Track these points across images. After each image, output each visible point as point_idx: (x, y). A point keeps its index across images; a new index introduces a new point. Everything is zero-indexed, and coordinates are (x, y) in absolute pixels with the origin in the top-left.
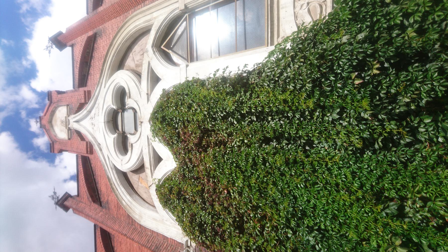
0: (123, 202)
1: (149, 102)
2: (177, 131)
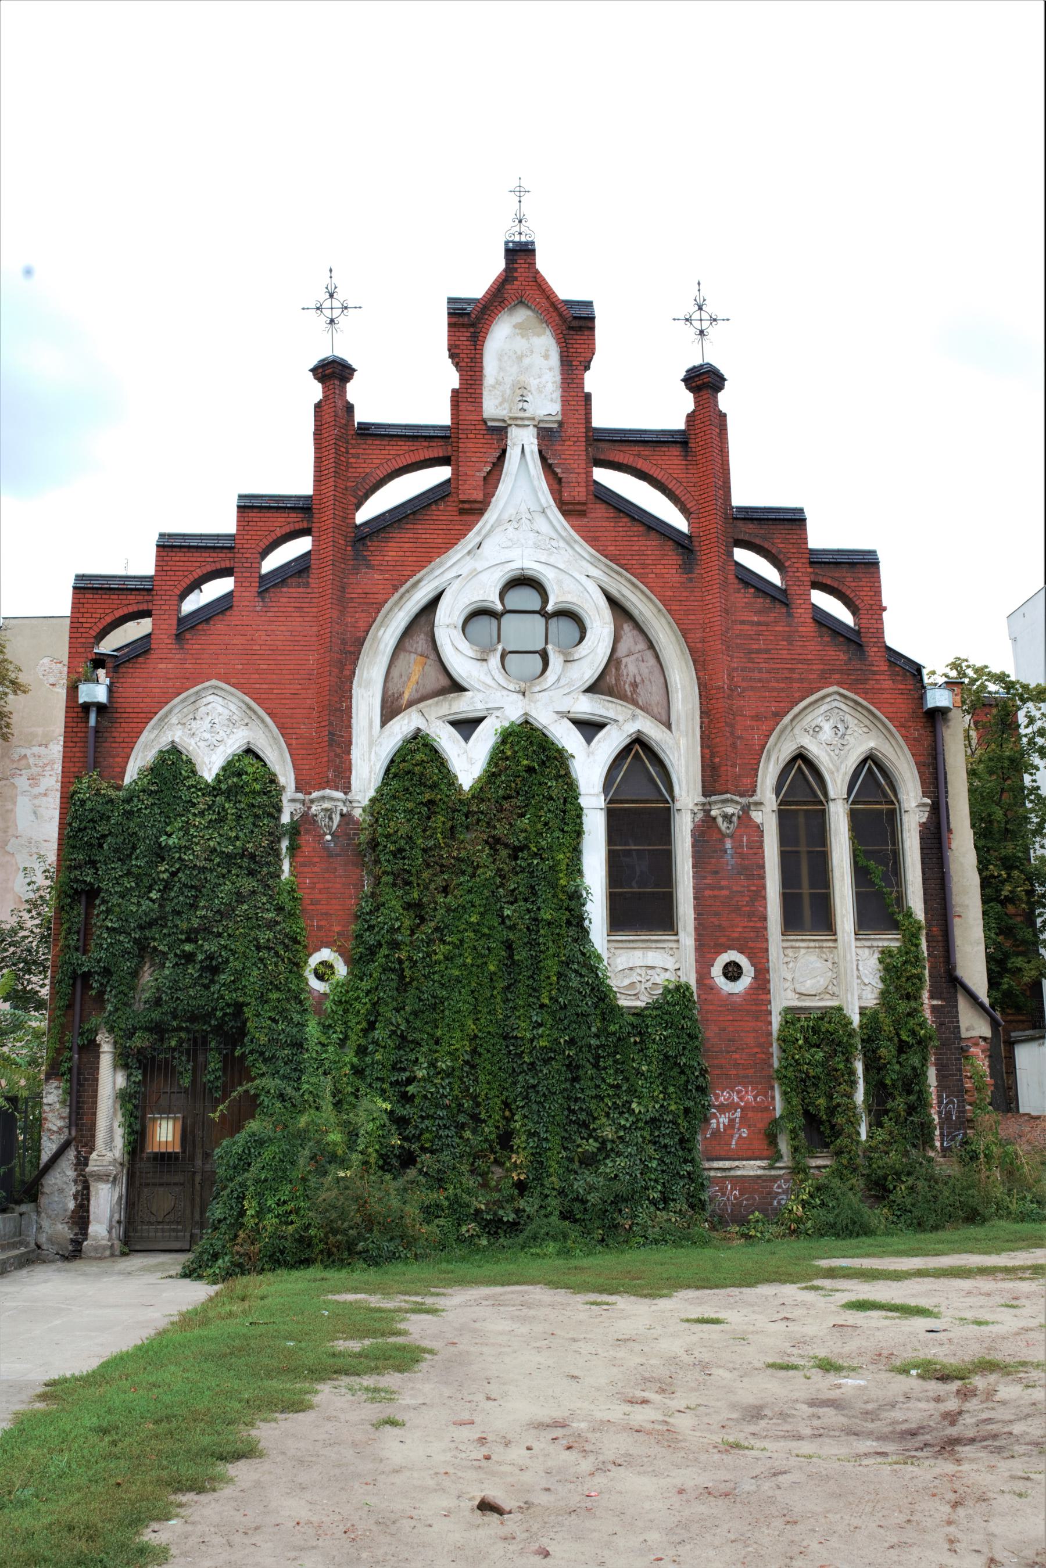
0: (383, 629)
1: (556, 717)
2: (514, 794)
